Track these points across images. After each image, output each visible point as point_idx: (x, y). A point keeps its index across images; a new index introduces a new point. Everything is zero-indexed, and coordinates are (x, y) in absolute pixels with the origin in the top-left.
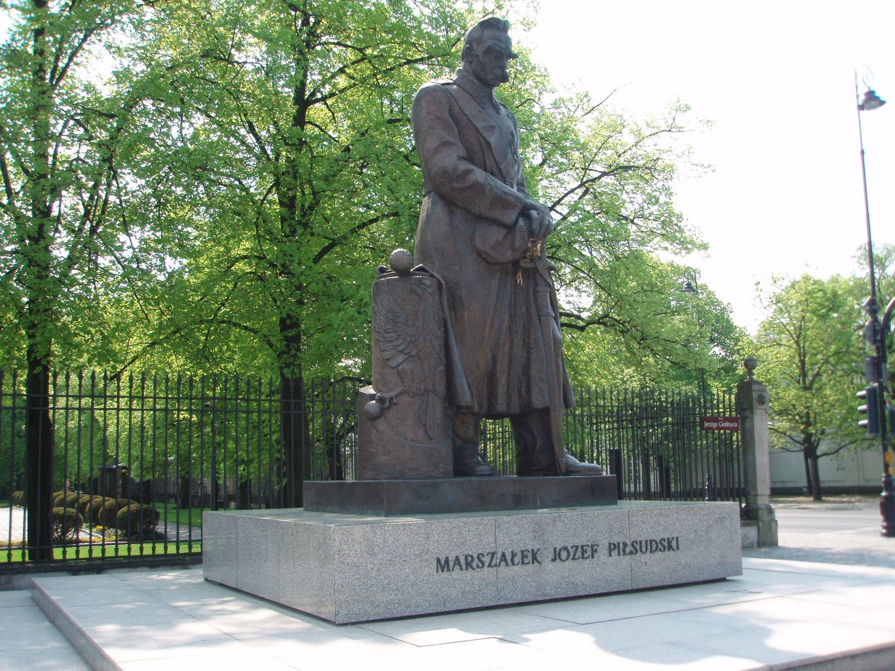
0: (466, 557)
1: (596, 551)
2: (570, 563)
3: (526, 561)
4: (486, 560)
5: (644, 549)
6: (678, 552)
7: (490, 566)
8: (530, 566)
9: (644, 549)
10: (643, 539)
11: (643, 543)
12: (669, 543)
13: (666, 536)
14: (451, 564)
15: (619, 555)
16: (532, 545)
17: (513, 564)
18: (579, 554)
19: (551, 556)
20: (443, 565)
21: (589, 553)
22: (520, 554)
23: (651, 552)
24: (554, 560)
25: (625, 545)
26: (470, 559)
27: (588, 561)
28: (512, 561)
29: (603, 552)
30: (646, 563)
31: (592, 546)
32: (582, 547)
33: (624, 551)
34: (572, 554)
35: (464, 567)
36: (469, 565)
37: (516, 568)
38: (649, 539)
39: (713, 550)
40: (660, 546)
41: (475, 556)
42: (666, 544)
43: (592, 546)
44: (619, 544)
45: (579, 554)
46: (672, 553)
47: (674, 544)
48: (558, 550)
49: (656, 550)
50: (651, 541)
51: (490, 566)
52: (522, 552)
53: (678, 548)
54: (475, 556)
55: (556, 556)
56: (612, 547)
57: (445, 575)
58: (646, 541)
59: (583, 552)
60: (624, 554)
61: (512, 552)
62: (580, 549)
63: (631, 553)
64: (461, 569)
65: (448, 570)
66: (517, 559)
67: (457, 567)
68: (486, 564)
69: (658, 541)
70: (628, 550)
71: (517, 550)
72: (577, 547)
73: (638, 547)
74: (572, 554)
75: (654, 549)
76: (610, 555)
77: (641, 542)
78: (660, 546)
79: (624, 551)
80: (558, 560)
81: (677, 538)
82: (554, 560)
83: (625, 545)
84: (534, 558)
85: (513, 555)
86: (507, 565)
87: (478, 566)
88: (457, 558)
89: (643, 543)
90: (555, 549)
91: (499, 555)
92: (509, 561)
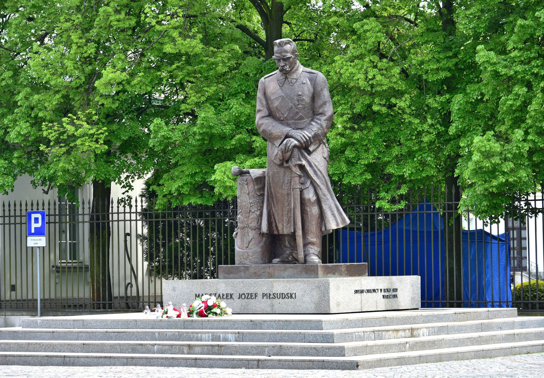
2: (246, 300)
6: (296, 300)
10: (279, 292)
11: (279, 295)
12: (291, 295)
13: (290, 292)
16: (230, 292)
18: (249, 296)
19: (238, 297)
21: (254, 296)
24: (239, 298)
29: (260, 296)
42: (289, 295)
45: (249, 296)
46: (292, 300)
47: (293, 296)
55: (240, 297)
66: (225, 297)
70: (271, 297)
71: (225, 294)
82: (239, 298)
83: (270, 295)
84: (231, 297)
85: (223, 295)
89: (279, 295)
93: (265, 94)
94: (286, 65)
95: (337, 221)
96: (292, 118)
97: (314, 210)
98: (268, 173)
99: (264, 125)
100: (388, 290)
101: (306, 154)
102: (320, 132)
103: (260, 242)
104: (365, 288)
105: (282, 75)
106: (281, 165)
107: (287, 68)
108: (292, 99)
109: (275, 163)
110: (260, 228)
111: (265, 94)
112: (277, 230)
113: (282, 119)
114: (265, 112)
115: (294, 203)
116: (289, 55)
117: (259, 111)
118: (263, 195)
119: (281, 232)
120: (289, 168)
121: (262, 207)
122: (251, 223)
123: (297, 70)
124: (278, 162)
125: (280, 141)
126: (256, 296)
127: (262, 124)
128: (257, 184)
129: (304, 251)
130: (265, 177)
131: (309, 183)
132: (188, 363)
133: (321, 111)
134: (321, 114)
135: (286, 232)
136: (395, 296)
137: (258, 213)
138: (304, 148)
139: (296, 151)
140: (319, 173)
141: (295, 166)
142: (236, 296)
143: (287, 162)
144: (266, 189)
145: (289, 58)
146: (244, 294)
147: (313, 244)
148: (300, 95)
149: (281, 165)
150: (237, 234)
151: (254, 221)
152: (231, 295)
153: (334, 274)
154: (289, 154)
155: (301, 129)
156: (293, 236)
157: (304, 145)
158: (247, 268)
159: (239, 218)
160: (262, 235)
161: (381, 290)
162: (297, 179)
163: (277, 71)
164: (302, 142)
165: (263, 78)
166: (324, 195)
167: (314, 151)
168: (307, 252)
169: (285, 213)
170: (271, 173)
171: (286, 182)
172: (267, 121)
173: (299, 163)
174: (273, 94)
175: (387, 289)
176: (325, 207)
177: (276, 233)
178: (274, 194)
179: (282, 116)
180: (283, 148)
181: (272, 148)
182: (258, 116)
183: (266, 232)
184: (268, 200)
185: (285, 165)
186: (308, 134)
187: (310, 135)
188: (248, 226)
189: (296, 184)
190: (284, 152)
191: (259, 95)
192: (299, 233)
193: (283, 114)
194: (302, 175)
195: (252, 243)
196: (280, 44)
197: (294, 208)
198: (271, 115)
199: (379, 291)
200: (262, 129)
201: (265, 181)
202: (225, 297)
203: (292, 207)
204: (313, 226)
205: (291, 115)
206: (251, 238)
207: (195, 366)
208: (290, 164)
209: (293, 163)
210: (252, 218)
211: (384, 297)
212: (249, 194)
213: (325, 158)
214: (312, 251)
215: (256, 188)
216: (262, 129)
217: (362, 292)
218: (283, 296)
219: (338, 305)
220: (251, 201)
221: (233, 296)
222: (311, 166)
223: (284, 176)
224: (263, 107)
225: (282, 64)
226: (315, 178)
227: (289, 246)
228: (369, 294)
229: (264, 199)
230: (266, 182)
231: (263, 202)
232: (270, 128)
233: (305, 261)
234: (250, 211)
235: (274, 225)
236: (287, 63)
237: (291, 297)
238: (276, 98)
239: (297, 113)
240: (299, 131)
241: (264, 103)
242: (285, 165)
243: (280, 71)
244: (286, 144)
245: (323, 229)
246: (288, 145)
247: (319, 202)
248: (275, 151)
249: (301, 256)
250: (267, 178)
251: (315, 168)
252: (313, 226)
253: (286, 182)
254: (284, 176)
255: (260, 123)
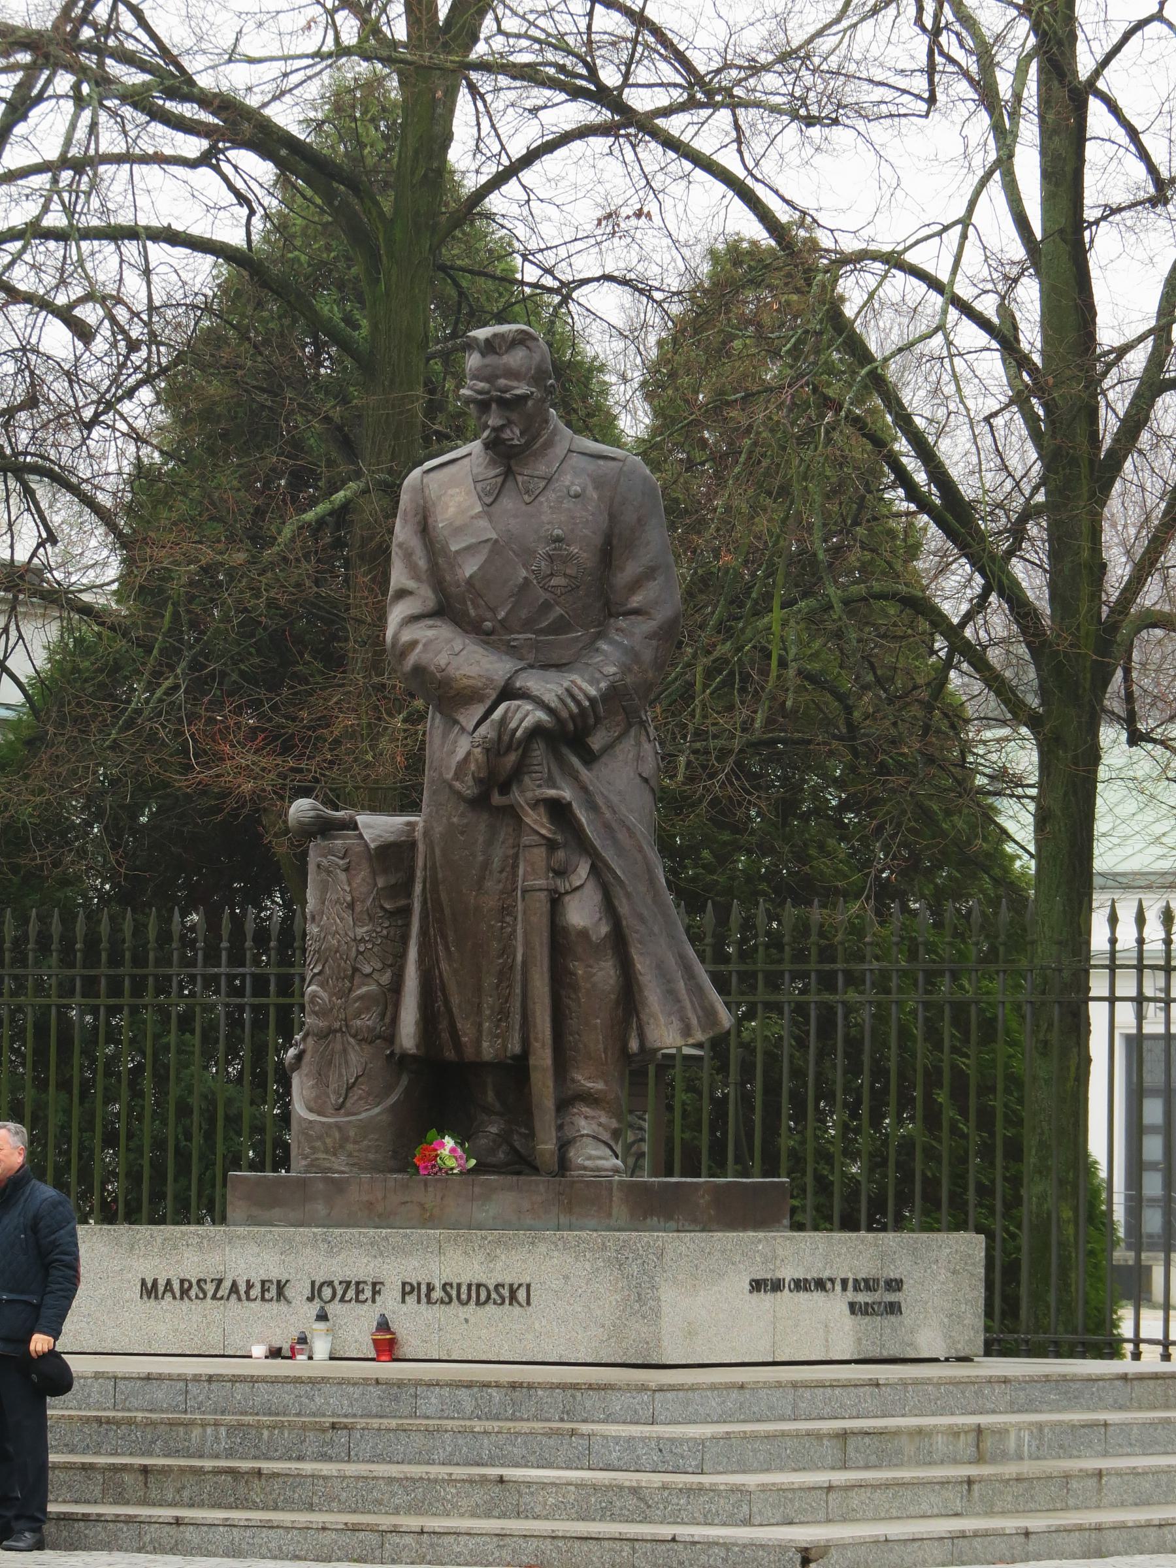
0: (182, 1281)
1: (379, 1292)
3: (267, 1296)
4: (210, 1288)
5: (464, 1297)
7: (214, 1297)
8: (274, 1304)
9: (464, 1297)
10: (465, 1279)
11: (464, 1289)
13: (508, 1280)
14: (161, 1289)
15: (419, 1302)
16: (275, 1274)
17: (248, 1299)
18: (351, 1293)
19: (307, 1292)
20: (150, 1290)
21: (368, 1293)
22: (258, 1286)
23: (478, 1303)
25: (430, 1288)
26: (186, 1285)
27: (365, 1307)
28: (247, 1293)
30: (467, 1321)
31: (374, 1284)
32: (358, 1283)
33: (428, 1296)
34: (340, 1293)
35: (178, 1295)
36: (185, 1293)
37: (252, 1305)
38: (475, 1281)
39: (599, 1312)
40: (494, 1295)
41: (194, 1282)
42: (506, 1292)
43: (374, 1284)
44: (419, 1284)
45: (351, 1293)
46: (517, 1310)
47: (521, 1295)
48: (317, 1285)
49: (486, 1302)
50: (479, 1286)
51: (214, 1297)
52: (263, 1282)
53: (528, 1303)
54: (194, 1282)
56: (408, 1288)
57: (152, 1302)
58: (469, 1286)
59: (358, 1292)
60: (429, 1302)
61: (248, 1281)
62: (353, 1287)
63: (442, 1302)
64: (174, 1298)
65: (156, 1297)
66: (255, 1292)
67: (169, 1294)
68: (210, 1294)
69: (491, 1288)
70: (437, 1294)
72: (348, 1283)
73: (454, 1293)
74: (340, 1293)
75: (483, 1297)
76: (403, 1301)
77: (459, 1285)
78: (494, 1295)
79: (428, 1296)
80: (317, 1300)
81: (528, 1286)
83: (430, 1288)
85: (249, 1286)
86: (240, 1299)
87: (197, 1297)
88: (169, 1282)
89: (464, 1289)
90: (313, 1283)
91: (227, 1284)
92: (242, 1292)
93: (424, 528)
94: (510, 423)
95: (684, 1020)
96: (527, 625)
97: (605, 973)
98: (426, 834)
99: (420, 647)
100: (868, 1285)
101: (575, 761)
102: (629, 680)
103: (389, 1089)
104: (788, 1273)
105: (493, 463)
106: (480, 802)
107: (513, 435)
108: (526, 554)
109: (458, 794)
110: (390, 1037)
111: (424, 528)
112: (457, 1045)
113: (488, 624)
114: (424, 598)
115: (527, 944)
116: (522, 389)
117: (402, 594)
118: (405, 912)
119: (469, 1053)
120: (512, 814)
121: (403, 955)
122: (357, 1015)
123: (549, 444)
124: (467, 788)
125: (479, 710)
126: (375, 1293)
127: (413, 644)
128: (385, 871)
129: (560, 1128)
130: (413, 845)
131: (583, 870)
132: (147, 1538)
133: (636, 601)
134: (636, 612)
135: (488, 1050)
136: (893, 1309)
137: (386, 978)
138: (569, 736)
139: (539, 751)
140: (622, 836)
141: (536, 804)
142: (298, 1291)
143: (505, 789)
144: (418, 889)
145: (524, 398)
146: (330, 1284)
147: (591, 1099)
148: (558, 540)
149: (480, 802)
150: (299, 1057)
151: (368, 1009)
152: (281, 1287)
153: (669, 1217)
154: (512, 757)
155: (559, 667)
156: (517, 1069)
157: (571, 726)
158: (338, 1187)
159: (314, 995)
160: (401, 1062)
161: (844, 1282)
162: (540, 853)
163: (476, 446)
164: (565, 714)
165: (417, 472)
166: (641, 919)
167: (608, 748)
168: (570, 1133)
169: (490, 981)
170: (438, 829)
171: (496, 863)
172: (430, 633)
173: (552, 792)
174: (458, 531)
175: (866, 1281)
176: (641, 964)
177: (450, 1055)
178: (447, 911)
179: (489, 615)
180: (492, 735)
181: (445, 736)
182: (397, 613)
183: (414, 1051)
184: (424, 932)
185: (497, 799)
186: (585, 684)
187: (593, 692)
188: (346, 1029)
189: (533, 872)
190: (495, 750)
191: (403, 532)
192: (543, 1058)
193: (494, 610)
194: (559, 838)
195: (358, 1092)
196: (490, 347)
197: (524, 963)
198: (447, 608)
199: (838, 1287)
200: (411, 660)
201: (413, 859)
202: (255, 1292)
203: (519, 958)
204: (593, 1035)
205: (524, 614)
206: (355, 1070)
207: (173, 1550)
208: (517, 797)
209: (529, 795)
210: (361, 998)
211: (853, 1312)
212: (351, 906)
213: (646, 780)
214: (585, 1127)
215: (381, 883)
216: (411, 660)
217: (776, 1286)
218: (478, 1295)
219: (691, 1333)
220: (361, 931)
221: (288, 1292)
222: (592, 806)
223: (489, 843)
224: (417, 577)
225: (494, 420)
226: (609, 855)
227: (498, 1106)
228: (803, 1296)
229: (408, 925)
230: (420, 862)
231: (405, 940)
232: (442, 660)
233: (564, 1165)
234: (355, 970)
235: (444, 1024)
236: (514, 416)
237: (513, 1297)
238: (468, 548)
239: (546, 607)
240: (552, 674)
241: (422, 563)
242: (497, 799)
243: (488, 446)
244: (503, 721)
245: (634, 1045)
246: (513, 725)
247: (619, 941)
248: (456, 748)
249: (547, 1145)
250: (421, 847)
251: (608, 815)
252: (593, 1035)
253: (496, 863)
254: (489, 843)
255: (406, 636)
